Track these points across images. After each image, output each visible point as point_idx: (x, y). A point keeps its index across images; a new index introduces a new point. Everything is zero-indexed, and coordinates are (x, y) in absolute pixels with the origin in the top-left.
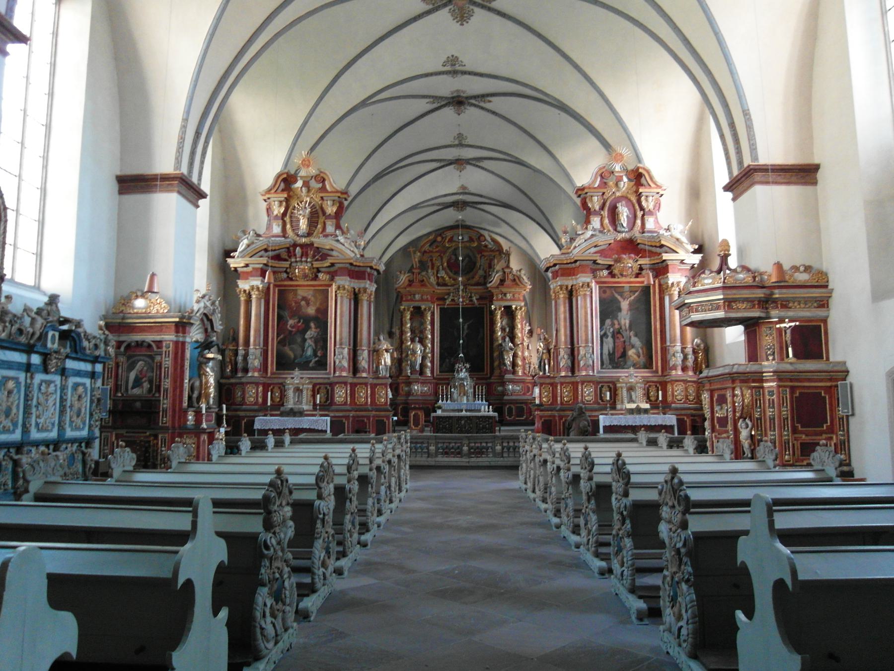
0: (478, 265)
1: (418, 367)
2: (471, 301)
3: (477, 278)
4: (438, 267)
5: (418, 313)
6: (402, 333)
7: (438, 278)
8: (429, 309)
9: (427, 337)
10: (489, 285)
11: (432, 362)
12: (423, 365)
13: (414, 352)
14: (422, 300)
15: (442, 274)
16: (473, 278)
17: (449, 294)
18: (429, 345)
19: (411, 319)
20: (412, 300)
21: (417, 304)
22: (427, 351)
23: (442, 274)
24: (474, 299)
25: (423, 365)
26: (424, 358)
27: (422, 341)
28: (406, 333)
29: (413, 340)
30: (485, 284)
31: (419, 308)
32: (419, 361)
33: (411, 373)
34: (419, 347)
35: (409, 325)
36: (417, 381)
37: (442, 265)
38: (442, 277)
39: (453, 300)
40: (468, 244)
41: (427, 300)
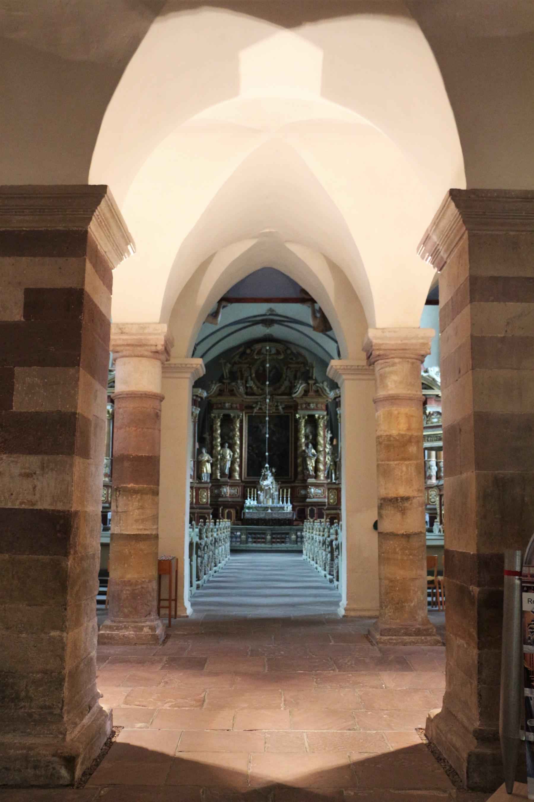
0: (284, 376)
1: (227, 471)
2: (277, 409)
3: (283, 388)
4: (247, 378)
5: (227, 421)
6: (213, 439)
7: (247, 388)
8: (238, 417)
9: (235, 443)
10: (294, 396)
11: (240, 466)
12: (232, 470)
13: (224, 457)
14: (232, 408)
15: (251, 384)
16: (279, 388)
17: (256, 403)
18: (238, 451)
19: (221, 426)
20: (222, 408)
21: (226, 412)
22: (236, 456)
23: (251, 384)
24: (280, 408)
25: (232, 470)
26: (233, 463)
27: (232, 447)
28: (216, 439)
29: (222, 446)
30: (290, 394)
31: (229, 415)
32: (228, 465)
33: (221, 477)
34: (228, 451)
35: (219, 432)
36: (226, 484)
37: (251, 375)
38: (251, 387)
39: (260, 409)
40: (275, 357)
41: (236, 408)
